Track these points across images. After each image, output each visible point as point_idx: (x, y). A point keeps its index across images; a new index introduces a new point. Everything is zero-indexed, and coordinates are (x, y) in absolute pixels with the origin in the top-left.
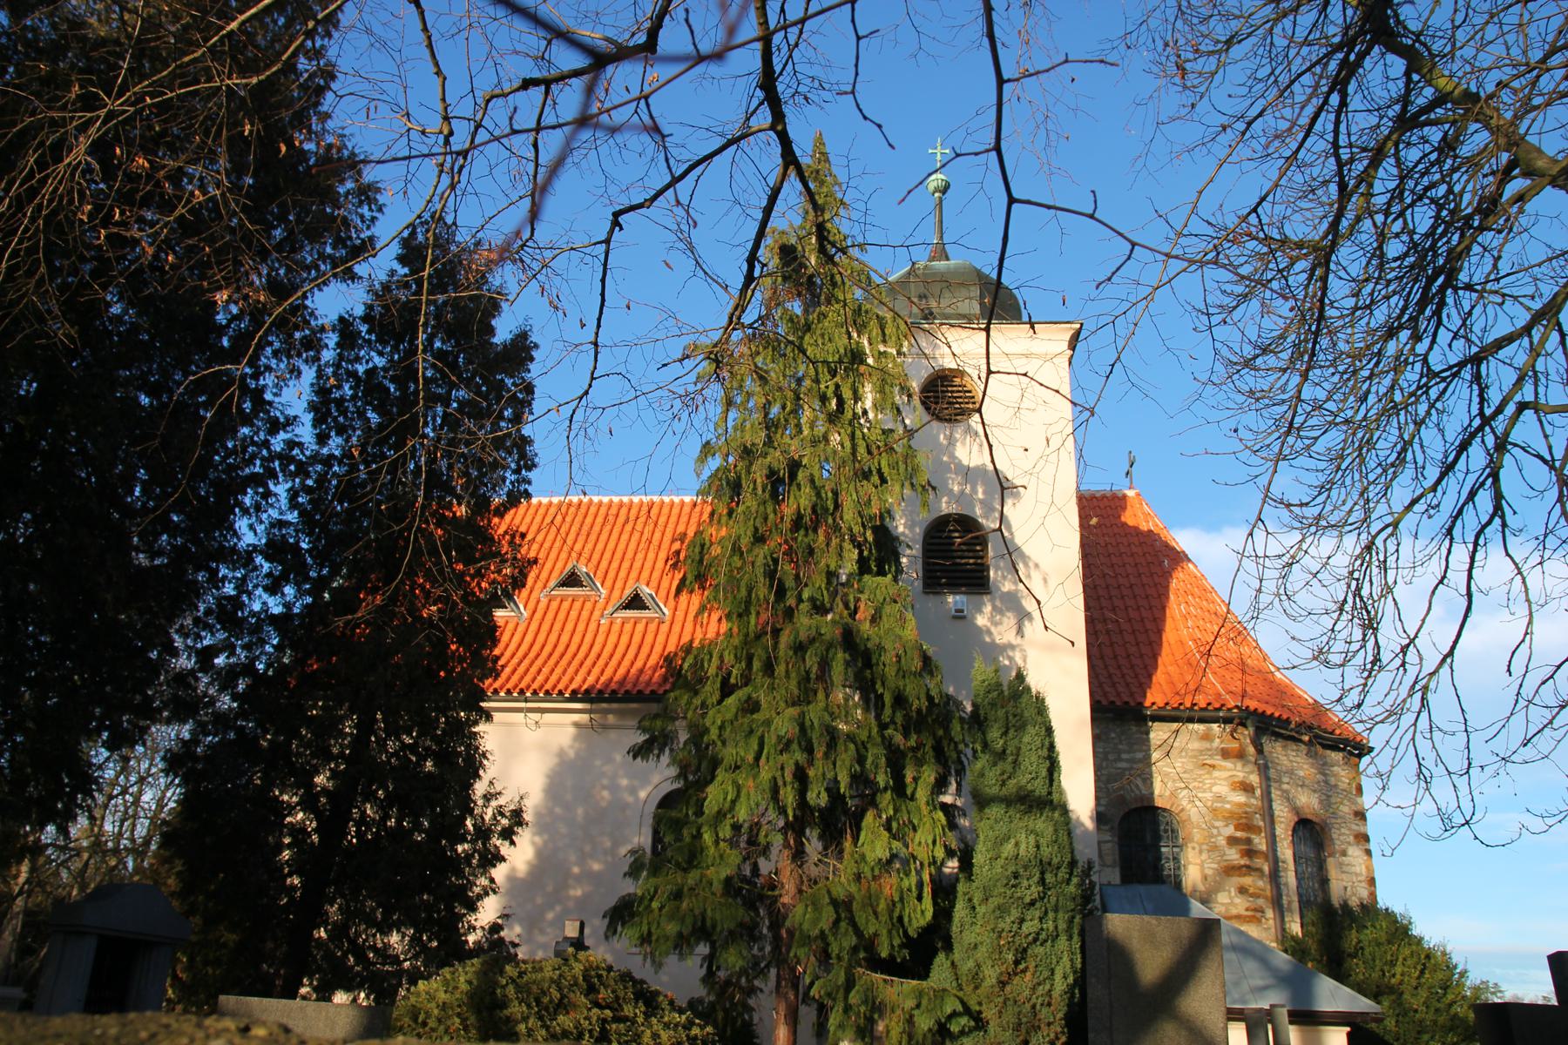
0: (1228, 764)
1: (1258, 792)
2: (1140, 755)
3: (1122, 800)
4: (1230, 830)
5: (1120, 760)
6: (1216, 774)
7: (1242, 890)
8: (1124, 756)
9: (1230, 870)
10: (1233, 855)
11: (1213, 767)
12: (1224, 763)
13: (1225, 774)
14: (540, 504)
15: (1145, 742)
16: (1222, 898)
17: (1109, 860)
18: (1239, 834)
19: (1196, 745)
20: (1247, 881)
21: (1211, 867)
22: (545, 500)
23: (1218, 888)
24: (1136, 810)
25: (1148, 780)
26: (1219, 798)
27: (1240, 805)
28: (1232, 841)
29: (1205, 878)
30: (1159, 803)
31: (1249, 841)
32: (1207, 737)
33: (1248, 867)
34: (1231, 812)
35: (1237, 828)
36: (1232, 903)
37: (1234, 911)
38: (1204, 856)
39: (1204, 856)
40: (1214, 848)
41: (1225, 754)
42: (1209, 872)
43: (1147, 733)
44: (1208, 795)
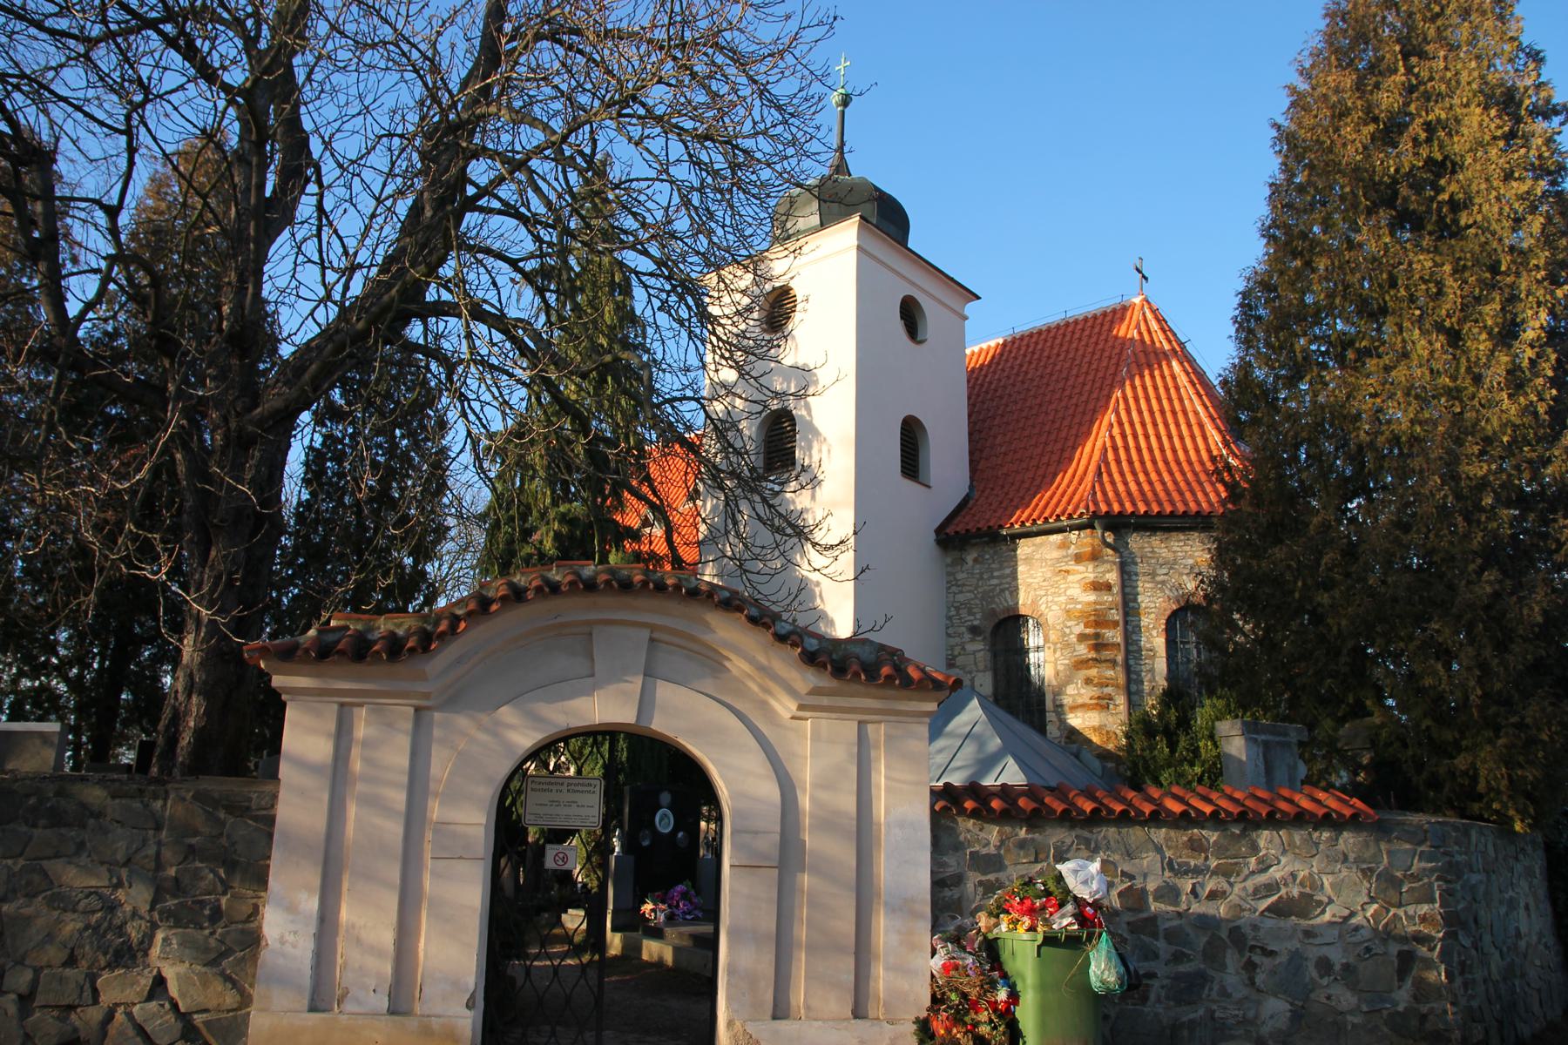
0: (1080, 568)
1: (1115, 590)
2: (1008, 571)
4: (1080, 629)
6: (1070, 578)
7: (1088, 681)
9: (1081, 664)
10: (1083, 650)
11: (1067, 572)
13: (1080, 576)
14: (973, 353)
15: (1014, 559)
16: (1071, 690)
17: (981, 666)
18: (1088, 631)
19: (1056, 554)
20: (1093, 672)
21: (1064, 662)
22: (976, 349)
23: (1069, 681)
24: (1005, 619)
25: (1015, 591)
26: (1072, 600)
27: (1089, 604)
28: (1082, 637)
29: (1057, 673)
30: (1023, 611)
32: (1064, 545)
33: (1095, 660)
34: (1081, 611)
36: (1079, 694)
37: (1080, 701)
38: (1058, 654)
39: (1058, 654)
40: (1068, 645)
41: (1078, 558)
42: (1060, 668)
43: (1015, 550)
44: (1063, 599)
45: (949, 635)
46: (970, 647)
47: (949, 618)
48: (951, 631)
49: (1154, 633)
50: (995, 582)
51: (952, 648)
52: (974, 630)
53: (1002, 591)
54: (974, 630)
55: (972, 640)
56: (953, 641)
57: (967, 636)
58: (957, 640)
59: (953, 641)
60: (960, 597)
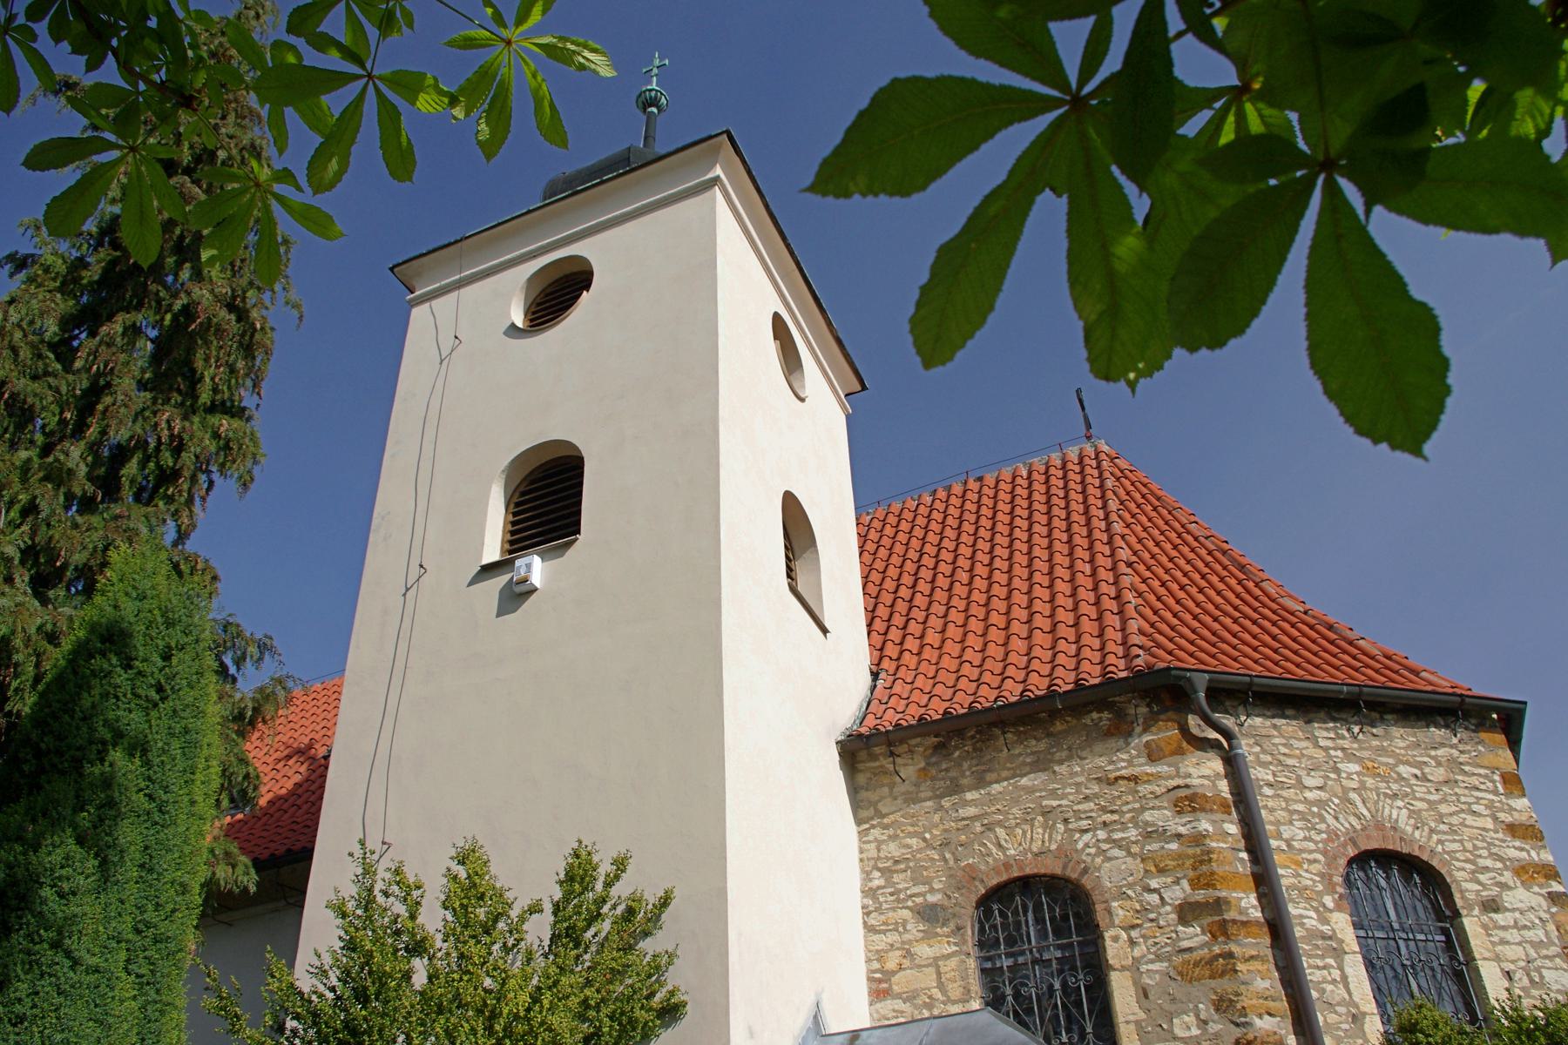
0: (1163, 769)
3: (972, 874)
4: (1179, 892)
5: (966, 803)
6: (1144, 789)
8: (969, 796)
11: (1134, 779)
12: (1149, 769)
18: (1200, 895)
28: (1187, 912)
31: (1218, 905)
34: (1180, 856)
35: (1195, 884)
45: (869, 929)
46: (925, 951)
47: (869, 892)
48: (874, 920)
49: (1329, 901)
50: (971, 811)
51: (880, 956)
52: (929, 914)
53: (989, 828)
54: (929, 914)
55: (928, 936)
56: (881, 941)
57: (915, 928)
58: (893, 937)
59: (881, 941)
60: (893, 849)
